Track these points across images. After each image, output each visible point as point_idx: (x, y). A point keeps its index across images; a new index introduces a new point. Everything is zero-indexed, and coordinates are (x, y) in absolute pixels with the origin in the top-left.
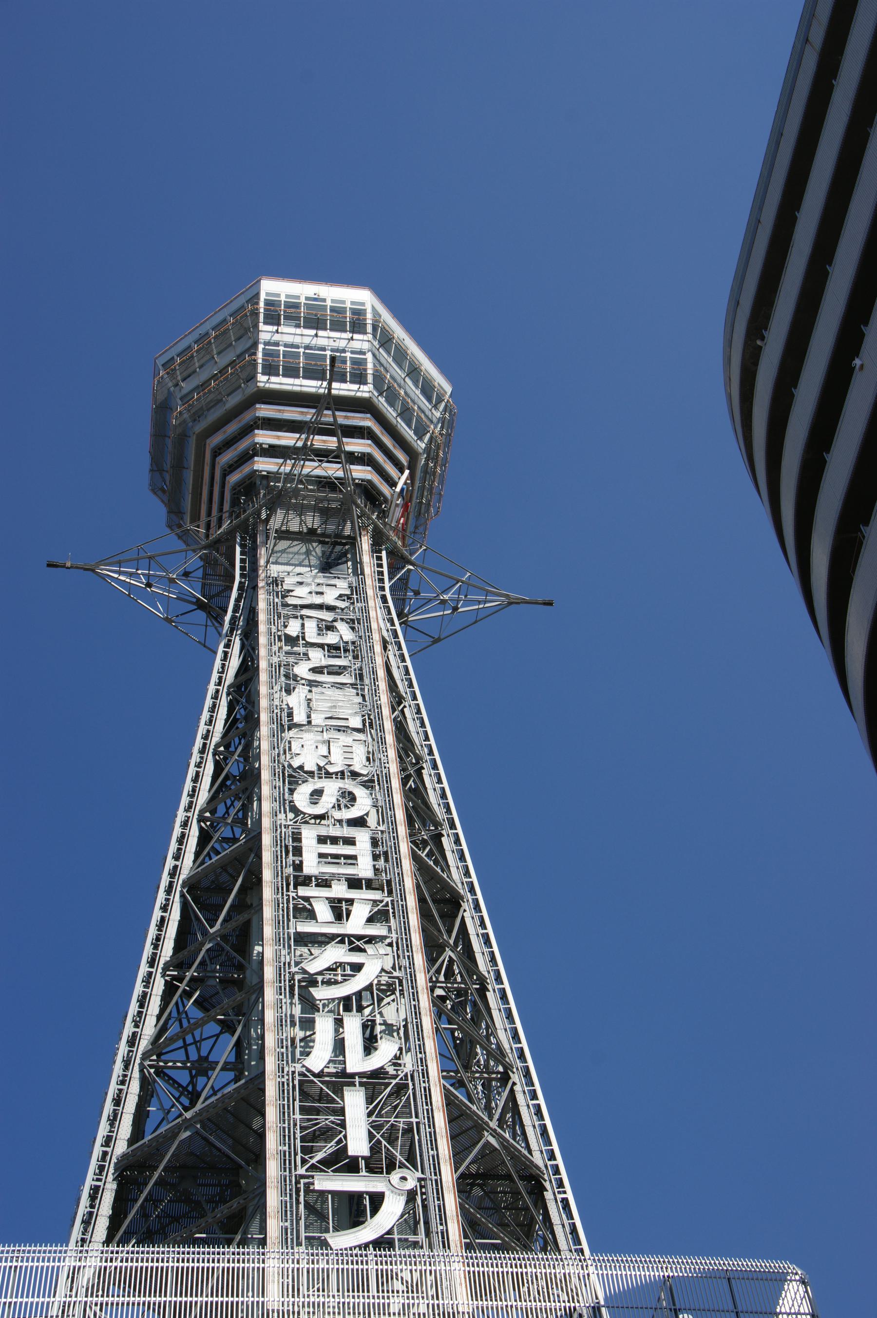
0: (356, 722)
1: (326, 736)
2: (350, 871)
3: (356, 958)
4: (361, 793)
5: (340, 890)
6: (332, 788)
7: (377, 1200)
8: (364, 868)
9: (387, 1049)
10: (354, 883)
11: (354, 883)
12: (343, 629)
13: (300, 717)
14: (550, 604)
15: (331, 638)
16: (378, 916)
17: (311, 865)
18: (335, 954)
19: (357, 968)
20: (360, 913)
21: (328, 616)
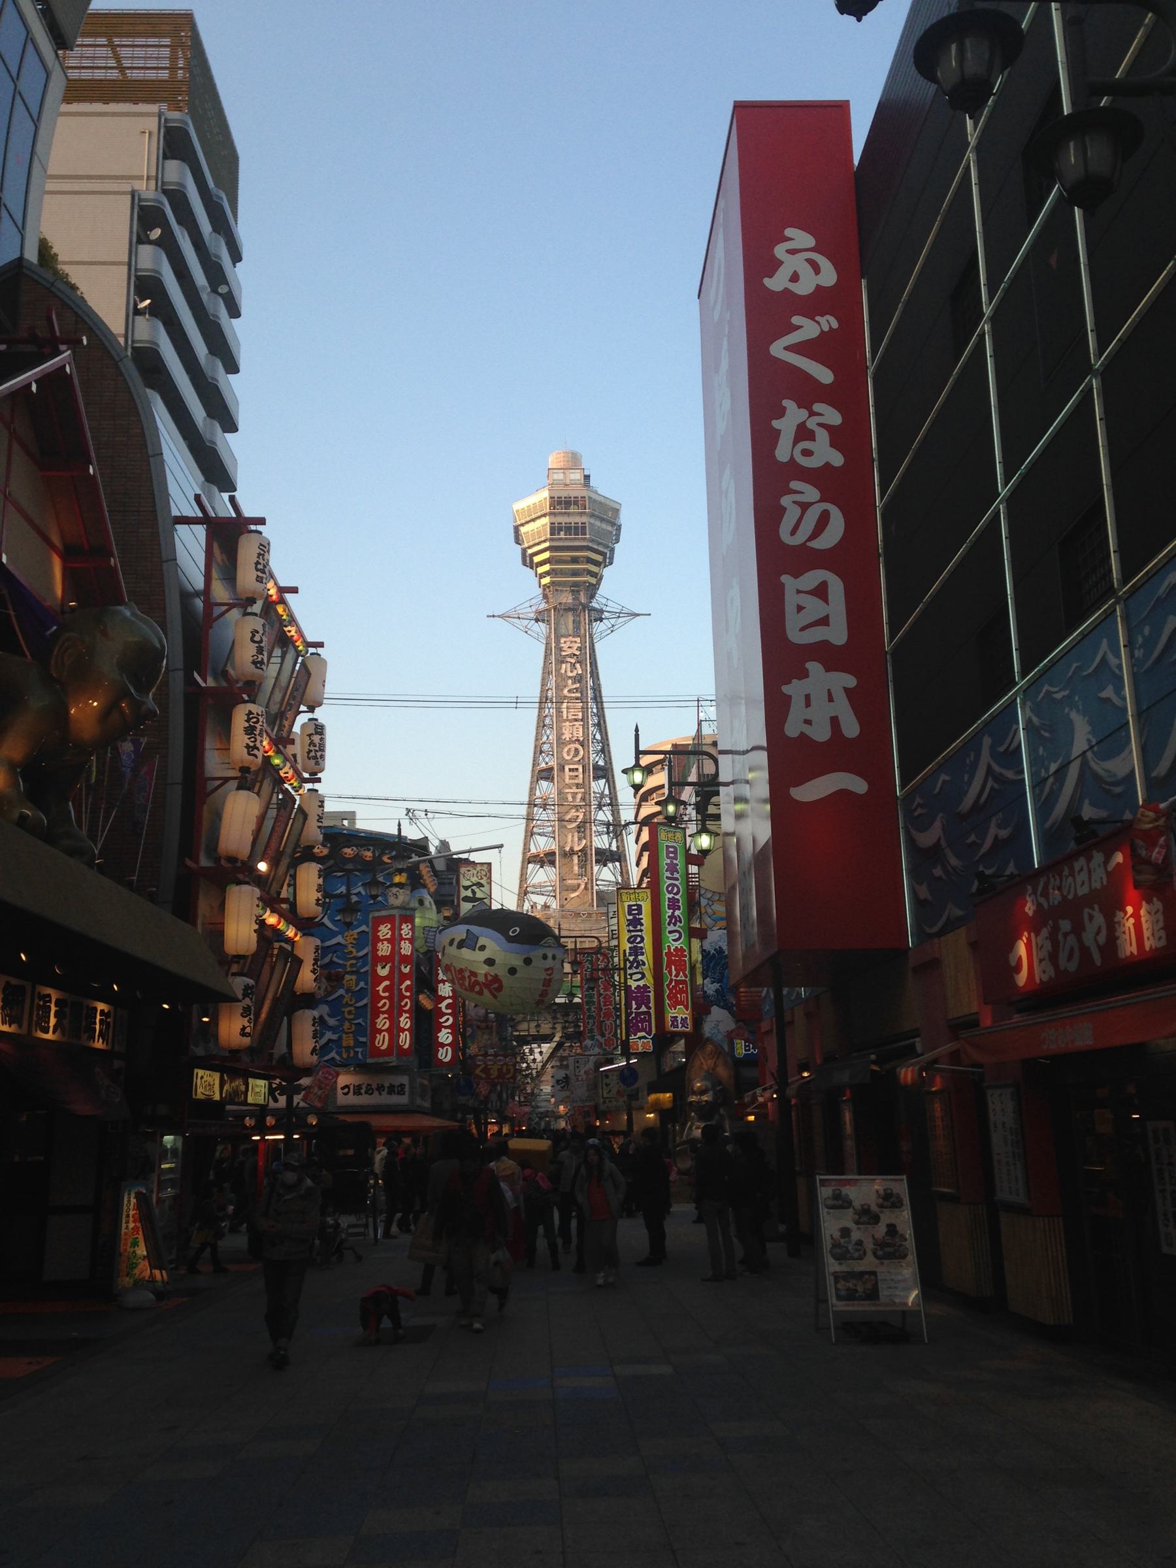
0: (580, 716)
1: (571, 724)
2: (576, 781)
3: (578, 814)
4: (580, 748)
5: (574, 790)
6: (573, 746)
7: (579, 885)
8: (581, 781)
9: (584, 842)
10: (578, 786)
11: (578, 786)
12: (578, 666)
13: (565, 717)
14: (650, 615)
15: (574, 674)
16: (583, 799)
17: (567, 781)
18: (573, 813)
19: (578, 816)
20: (579, 796)
21: (573, 661)
